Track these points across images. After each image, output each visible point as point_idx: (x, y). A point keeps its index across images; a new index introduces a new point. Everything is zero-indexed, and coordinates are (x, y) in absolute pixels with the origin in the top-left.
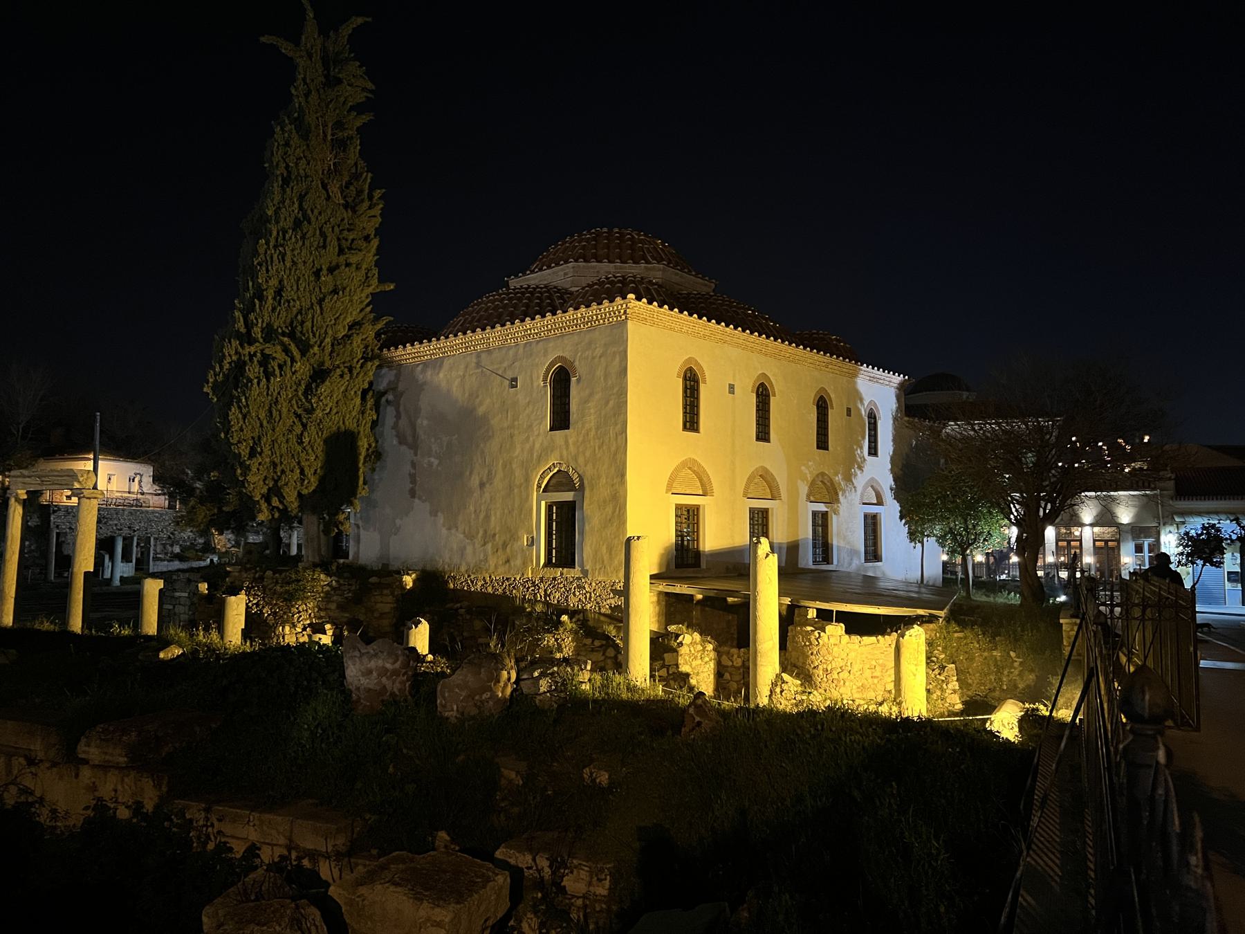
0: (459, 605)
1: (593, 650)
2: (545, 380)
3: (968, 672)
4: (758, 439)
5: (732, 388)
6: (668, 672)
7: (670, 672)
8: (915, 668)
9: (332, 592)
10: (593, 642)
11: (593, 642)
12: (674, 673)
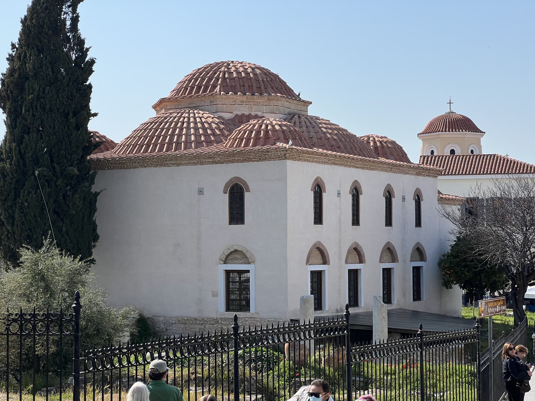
2: (225, 192)
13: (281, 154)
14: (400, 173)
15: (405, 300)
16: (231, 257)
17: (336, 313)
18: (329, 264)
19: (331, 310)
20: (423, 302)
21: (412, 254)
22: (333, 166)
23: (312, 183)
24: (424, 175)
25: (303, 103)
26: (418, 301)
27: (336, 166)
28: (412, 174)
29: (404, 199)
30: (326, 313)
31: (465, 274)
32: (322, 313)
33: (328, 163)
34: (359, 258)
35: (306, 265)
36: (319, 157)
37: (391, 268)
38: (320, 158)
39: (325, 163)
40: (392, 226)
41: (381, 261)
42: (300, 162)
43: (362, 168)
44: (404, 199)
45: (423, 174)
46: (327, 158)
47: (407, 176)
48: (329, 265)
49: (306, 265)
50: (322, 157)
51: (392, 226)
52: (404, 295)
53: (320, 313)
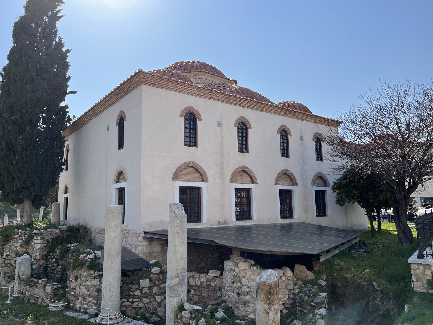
0: (72, 245)
1: (94, 278)
2: (117, 125)
3: (345, 296)
4: (241, 150)
5: (220, 125)
6: (141, 292)
7: (143, 292)
8: (268, 307)
9: (19, 238)
10: (95, 272)
11: (95, 272)
12: (146, 293)
13: (138, 80)
14: (296, 118)
15: (307, 216)
16: (121, 178)
17: (218, 225)
18: (208, 182)
19: (211, 222)
20: (328, 217)
21: (313, 180)
22: (211, 101)
23: (181, 110)
24: (323, 124)
25: (228, 81)
26: (323, 217)
27: (215, 102)
28: (311, 122)
29: (302, 138)
30: (203, 225)
31: (353, 193)
32: (199, 225)
33: (203, 97)
34: (251, 180)
35: (172, 180)
36: (188, 88)
37: (291, 190)
38: (191, 90)
39: (199, 96)
40: (289, 158)
41: (277, 183)
42: (162, 90)
43: (250, 108)
44: (302, 138)
45: (322, 123)
46: (201, 91)
47: (305, 122)
48: (208, 183)
49: (172, 180)
50: (192, 89)
51: (289, 158)
52: (306, 211)
53: (194, 225)
